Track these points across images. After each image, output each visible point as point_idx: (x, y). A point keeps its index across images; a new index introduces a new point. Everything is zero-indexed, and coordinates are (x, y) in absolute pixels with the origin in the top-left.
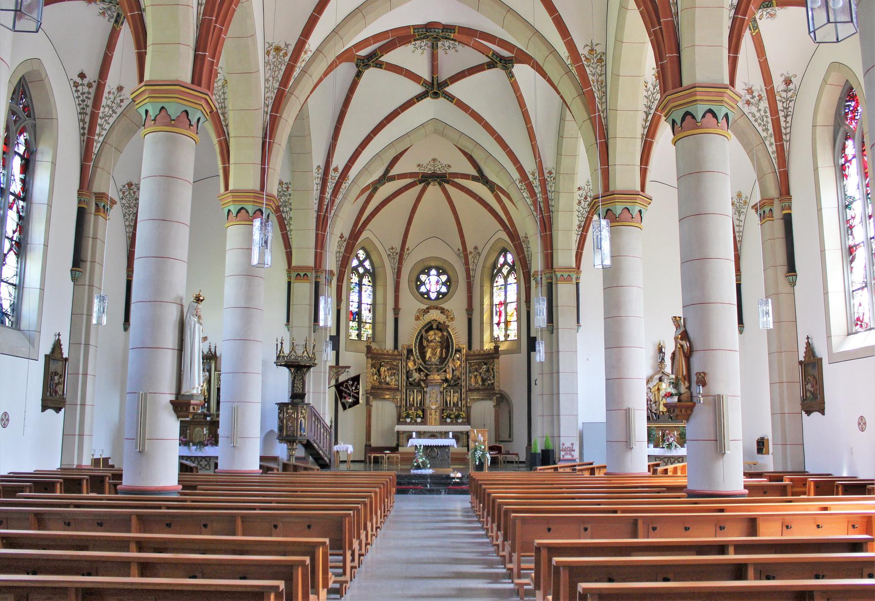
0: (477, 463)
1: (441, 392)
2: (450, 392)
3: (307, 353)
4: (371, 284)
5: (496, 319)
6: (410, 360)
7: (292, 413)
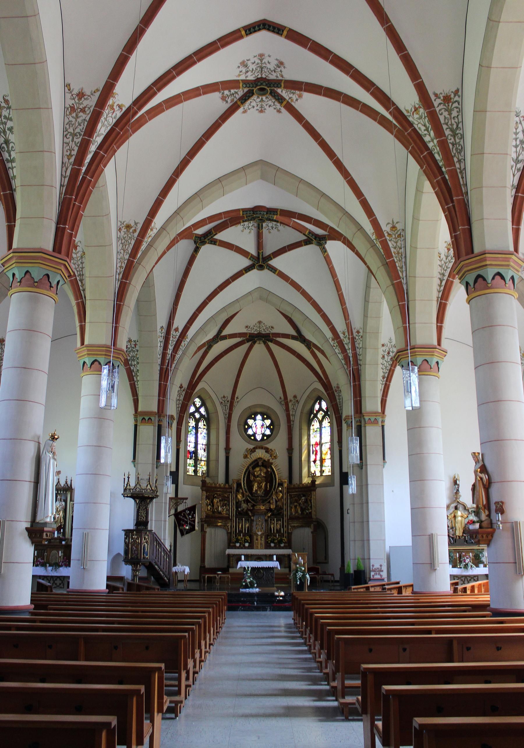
0: (298, 583)
1: (266, 521)
3: (150, 486)
4: (206, 427)
5: (313, 457)
6: (239, 492)
7: (137, 539)
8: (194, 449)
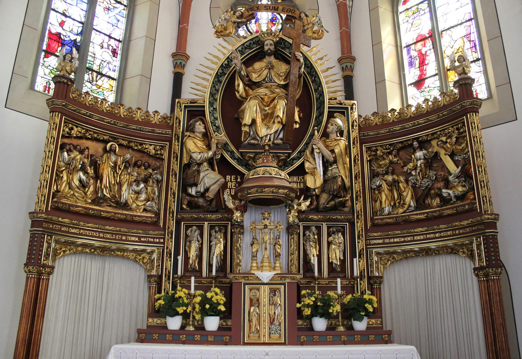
1: (290, 229)
2: (319, 228)
6: (193, 131)
8: (79, 38)
